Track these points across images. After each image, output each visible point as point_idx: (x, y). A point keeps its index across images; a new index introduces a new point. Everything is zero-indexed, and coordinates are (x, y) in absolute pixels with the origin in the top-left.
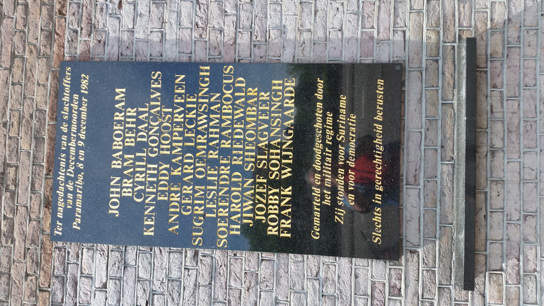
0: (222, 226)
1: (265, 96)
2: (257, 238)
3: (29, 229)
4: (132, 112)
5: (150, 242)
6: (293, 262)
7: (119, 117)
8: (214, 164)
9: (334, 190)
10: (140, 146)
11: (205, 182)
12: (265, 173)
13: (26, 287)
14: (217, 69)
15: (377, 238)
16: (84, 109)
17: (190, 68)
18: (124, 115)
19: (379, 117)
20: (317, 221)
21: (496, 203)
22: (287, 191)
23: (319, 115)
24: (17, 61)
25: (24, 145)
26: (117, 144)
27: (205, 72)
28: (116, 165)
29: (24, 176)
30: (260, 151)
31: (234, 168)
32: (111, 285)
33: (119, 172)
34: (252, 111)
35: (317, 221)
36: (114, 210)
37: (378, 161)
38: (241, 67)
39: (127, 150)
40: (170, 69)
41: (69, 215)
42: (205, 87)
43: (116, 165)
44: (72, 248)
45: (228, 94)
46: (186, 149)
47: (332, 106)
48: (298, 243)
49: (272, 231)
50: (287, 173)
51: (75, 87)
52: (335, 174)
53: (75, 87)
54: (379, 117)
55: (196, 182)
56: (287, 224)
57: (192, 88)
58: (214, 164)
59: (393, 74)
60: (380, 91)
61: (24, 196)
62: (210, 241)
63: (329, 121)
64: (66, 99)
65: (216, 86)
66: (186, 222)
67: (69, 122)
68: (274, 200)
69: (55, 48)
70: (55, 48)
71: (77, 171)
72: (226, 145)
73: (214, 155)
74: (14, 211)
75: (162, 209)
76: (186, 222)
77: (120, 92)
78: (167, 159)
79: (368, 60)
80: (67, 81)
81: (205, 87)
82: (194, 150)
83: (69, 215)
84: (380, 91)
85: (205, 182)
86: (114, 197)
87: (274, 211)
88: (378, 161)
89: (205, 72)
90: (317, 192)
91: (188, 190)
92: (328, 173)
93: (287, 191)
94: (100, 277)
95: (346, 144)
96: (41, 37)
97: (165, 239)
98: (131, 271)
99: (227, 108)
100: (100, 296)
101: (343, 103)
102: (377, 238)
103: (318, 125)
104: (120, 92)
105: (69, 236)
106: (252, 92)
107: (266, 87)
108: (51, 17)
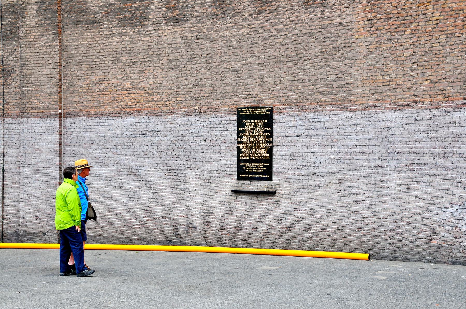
0: (241, 145)
1: (266, 153)
2: (239, 151)
3: (240, 102)
4: (262, 124)
5: (238, 129)
6: (236, 160)
7: (261, 121)
8: (253, 142)
9: (249, 167)
10: (256, 126)
11: (249, 140)
12: (251, 153)
13: (229, 103)
14: (271, 142)
15: (241, 176)
16: (263, 113)
17: (271, 136)
18: (261, 122)
19: (262, 176)
20: (243, 164)
21: (248, 198)
22: (248, 158)
23: (262, 164)
24: (273, 95)
25: (256, 99)
26: (256, 121)
27: (270, 139)
28: (252, 121)
29: (250, 100)
30: (255, 152)
31: (252, 147)
32: (230, 122)
33: (251, 122)
34: (263, 150)
35: (243, 164)
36: (243, 122)
37: (254, 176)
38: (271, 147)
39: (255, 123)
40: (271, 132)
41: (242, 112)
42: (267, 139)
43: (252, 121)
44: (236, 112)
45: (266, 145)
46: (255, 136)
47: (264, 166)
48: (239, 161)
49: (241, 155)
50: (251, 158)
51: (267, 111)
52: (251, 167)
53: (267, 111)
54: (262, 176)
55: (249, 139)
56: (242, 158)
57: (267, 137)
58: (253, 142)
59: (270, 179)
60: (267, 176)
61: (246, 100)
62: (239, 142)
63: (261, 166)
64: (265, 109)
65: (268, 142)
66: (241, 137)
67: (260, 110)
68: (246, 155)
69: (276, 104)
70: (276, 104)
71: (251, 113)
72: (256, 145)
73: (254, 142)
74: (243, 98)
75: (244, 132)
76: (241, 137)
77: (266, 121)
78: (253, 132)
79: (273, 174)
80: (268, 109)
81: (267, 139)
82: (255, 138)
83: (242, 112)
84: (267, 176)
85: (249, 140)
86: (246, 121)
87: (244, 155)
88: (254, 176)
89: (270, 139)
90: (248, 164)
91: (248, 137)
92: (252, 166)
93: (248, 158)
94: (232, 119)
95: (257, 170)
96: (278, 101)
97: (239, 132)
98: (233, 126)
99: (263, 145)
100: (228, 119)
101: (265, 169)
102: (241, 176)
103: (260, 164)
104: (266, 121)
105: (239, 112)
106: (267, 150)
107: (268, 153)
108: (283, 102)
